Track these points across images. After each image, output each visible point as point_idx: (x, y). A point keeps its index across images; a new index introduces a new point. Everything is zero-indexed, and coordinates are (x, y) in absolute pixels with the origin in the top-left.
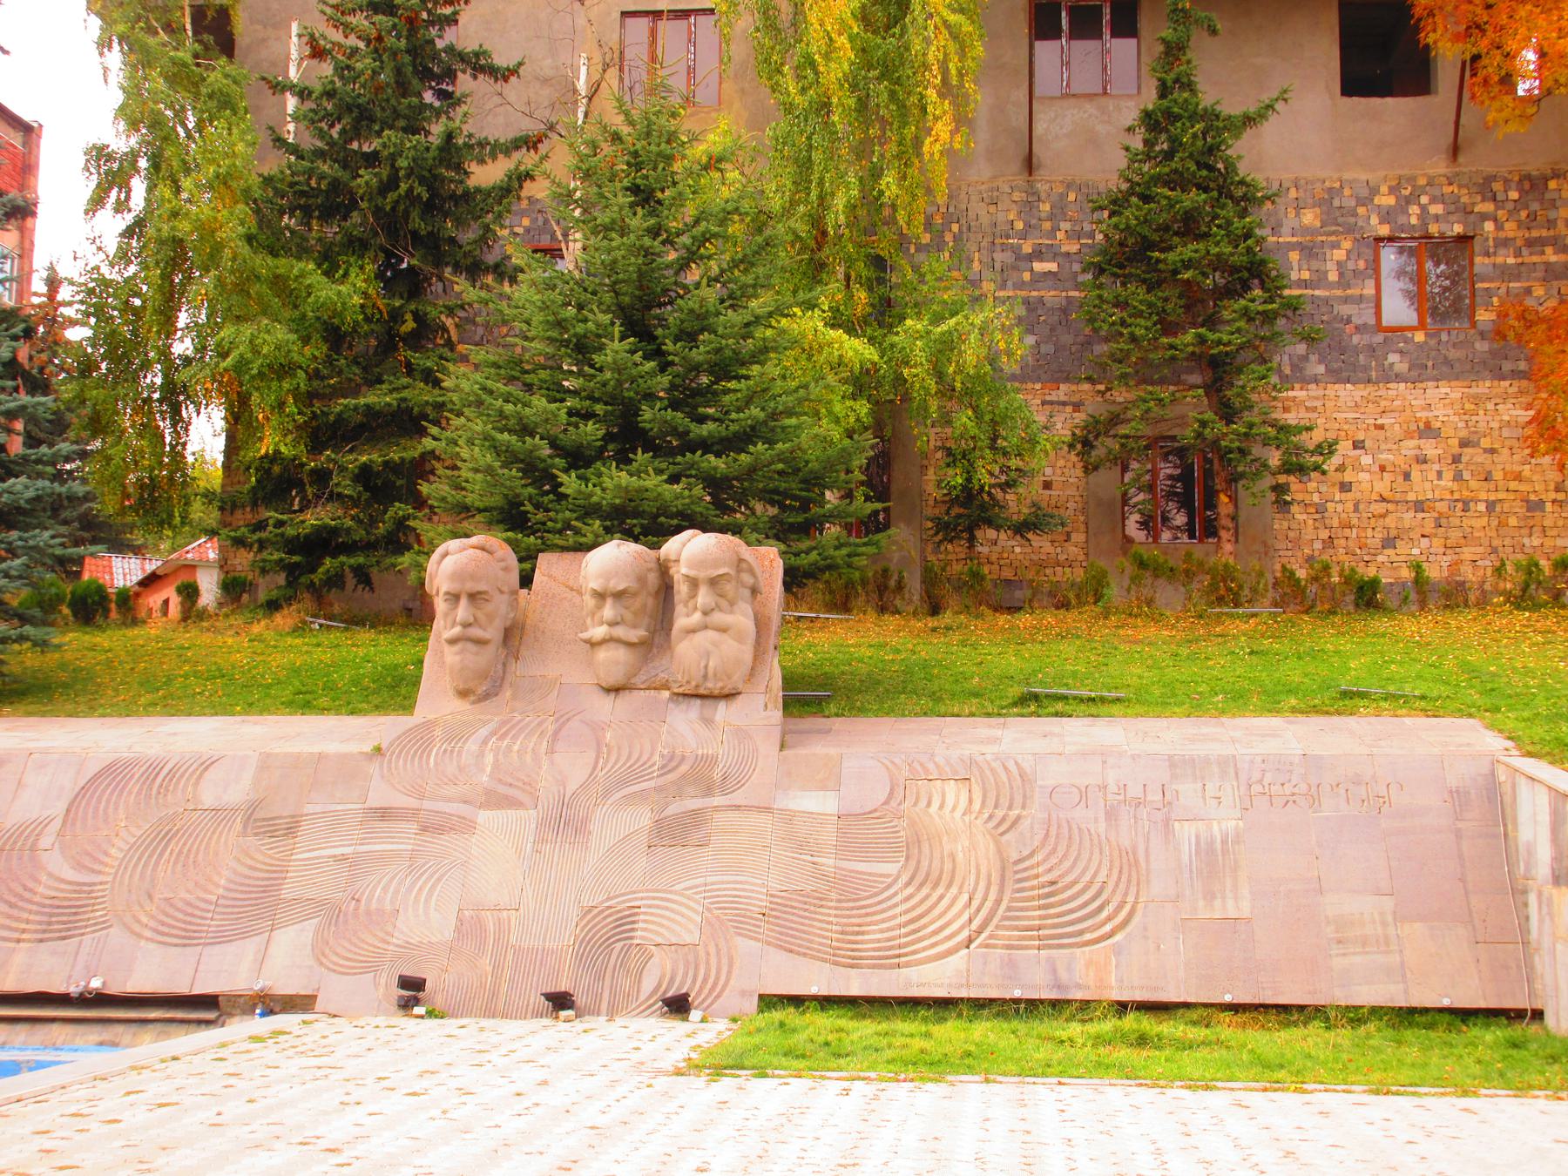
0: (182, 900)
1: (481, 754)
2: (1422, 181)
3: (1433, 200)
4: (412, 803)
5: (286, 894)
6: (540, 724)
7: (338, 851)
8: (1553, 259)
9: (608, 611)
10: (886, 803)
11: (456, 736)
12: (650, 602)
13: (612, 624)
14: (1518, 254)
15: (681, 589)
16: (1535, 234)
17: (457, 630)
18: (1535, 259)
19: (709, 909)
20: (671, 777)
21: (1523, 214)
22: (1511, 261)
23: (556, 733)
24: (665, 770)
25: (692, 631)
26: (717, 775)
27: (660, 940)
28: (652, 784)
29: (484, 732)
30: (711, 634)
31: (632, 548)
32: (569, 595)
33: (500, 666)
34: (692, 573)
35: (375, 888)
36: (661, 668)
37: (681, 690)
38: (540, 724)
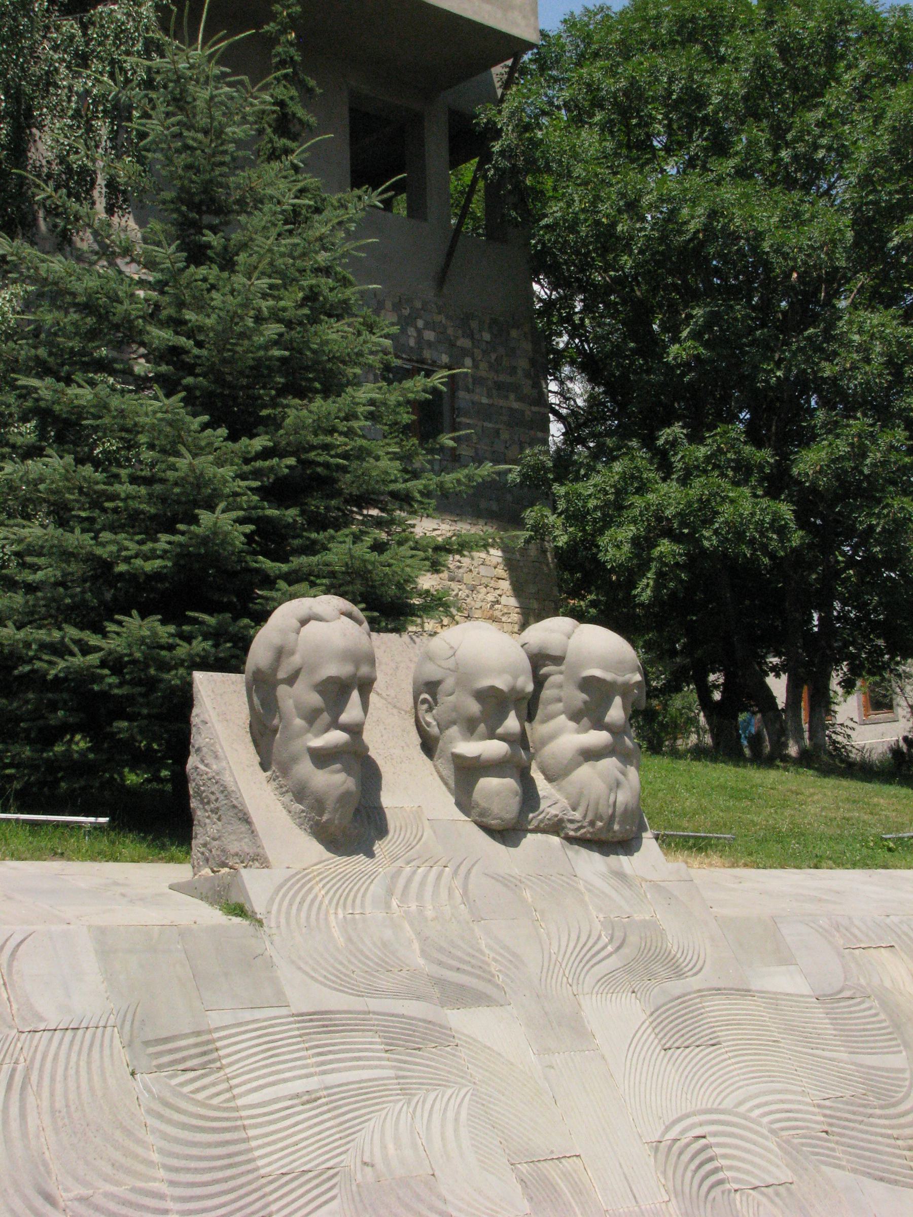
0: (106, 1195)
2: (418, 305)
3: (427, 326)
4: (357, 1003)
5: (268, 1165)
6: (439, 876)
7: (299, 1086)
8: (516, 405)
10: (846, 979)
14: (489, 396)
16: (503, 378)
18: (502, 402)
19: (773, 1132)
21: (493, 356)
22: (485, 400)
27: (757, 1183)
29: (377, 888)
34: (608, 676)
35: (384, 1147)
38: (439, 876)
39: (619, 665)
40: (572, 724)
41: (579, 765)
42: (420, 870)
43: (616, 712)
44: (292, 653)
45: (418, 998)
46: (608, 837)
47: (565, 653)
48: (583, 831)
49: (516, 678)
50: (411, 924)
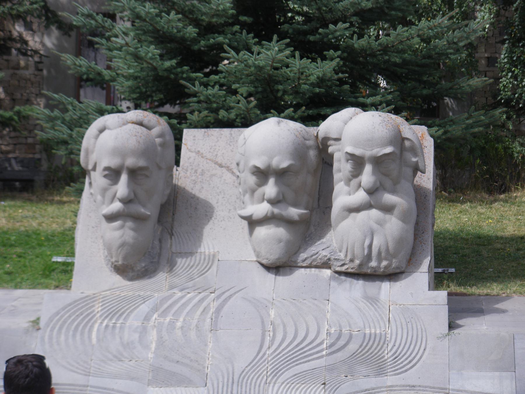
1: (144, 331)
9: (271, 189)
11: (117, 311)
12: (310, 180)
13: (273, 202)
15: (341, 168)
17: (117, 206)
20: (340, 356)
23: (218, 310)
24: (334, 348)
25: (357, 209)
26: (388, 355)
28: (322, 362)
29: (145, 308)
30: (374, 213)
31: (297, 126)
32: (219, 171)
33: (157, 243)
34: (358, 152)
36: (320, 249)
37: (343, 269)
39: (369, 142)
40: (346, 188)
41: (344, 218)
42: (189, 295)
43: (367, 176)
44: (93, 152)
45: (132, 379)
46: (391, 271)
47: (341, 134)
48: (346, 267)
49: (272, 158)
50: (159, 332)
